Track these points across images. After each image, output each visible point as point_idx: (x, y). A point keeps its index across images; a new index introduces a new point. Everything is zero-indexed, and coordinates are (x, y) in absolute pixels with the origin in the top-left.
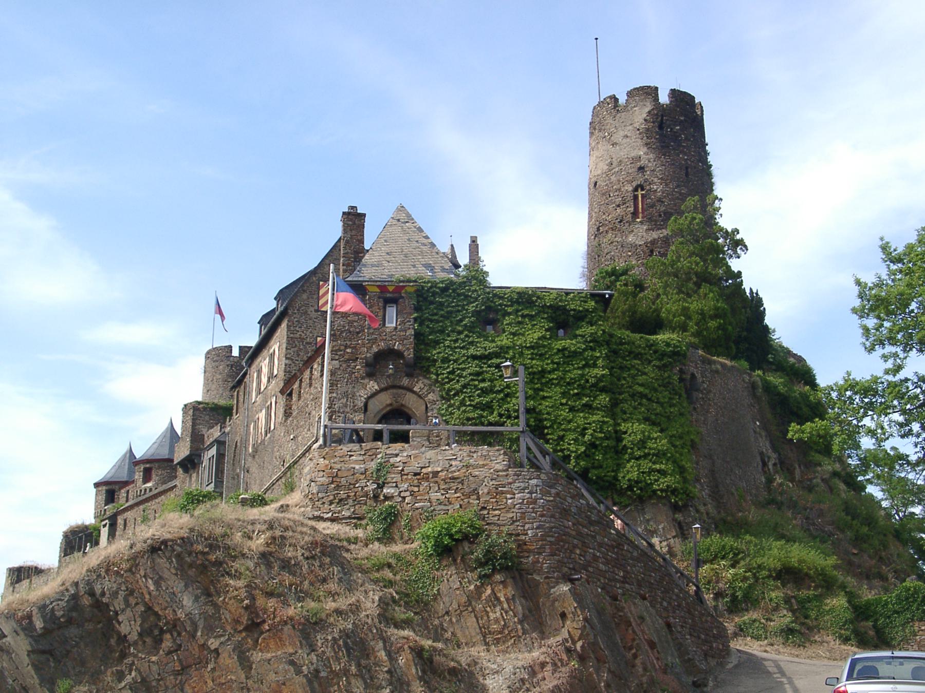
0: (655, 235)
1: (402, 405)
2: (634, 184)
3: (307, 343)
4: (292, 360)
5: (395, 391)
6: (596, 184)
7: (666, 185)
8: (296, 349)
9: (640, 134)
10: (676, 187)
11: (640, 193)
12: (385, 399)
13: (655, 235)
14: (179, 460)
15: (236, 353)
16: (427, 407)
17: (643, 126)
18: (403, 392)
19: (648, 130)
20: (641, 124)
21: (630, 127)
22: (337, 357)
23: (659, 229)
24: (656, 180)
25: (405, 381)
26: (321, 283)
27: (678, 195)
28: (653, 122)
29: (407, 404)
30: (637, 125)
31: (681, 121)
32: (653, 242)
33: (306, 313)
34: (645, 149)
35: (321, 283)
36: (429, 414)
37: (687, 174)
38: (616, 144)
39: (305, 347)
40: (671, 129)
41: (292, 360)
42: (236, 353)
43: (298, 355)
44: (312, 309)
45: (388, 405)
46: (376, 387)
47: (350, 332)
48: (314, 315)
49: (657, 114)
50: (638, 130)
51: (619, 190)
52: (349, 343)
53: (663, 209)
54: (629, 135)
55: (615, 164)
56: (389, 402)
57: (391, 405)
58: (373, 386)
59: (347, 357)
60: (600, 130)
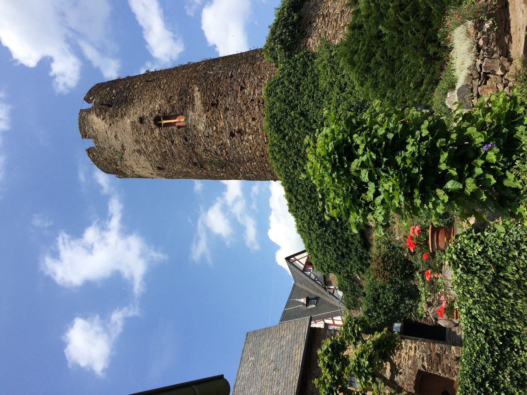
0: (198, 103)
2: (153, 126)
6: (159, 168)
10: (160, 87)
13: (198, 103)
19: (111, 116)
20: (106, 122)
21: (109, 133)
23: (193, 100)
24: (151, 106)
27: (166, 86)
30: (107, 126)
32: (204, 104)
34: (126, 117)
38: (123, 146)
40: (114, 96)
49: (100, 109)
50: (110, 125)
51: (159, 142)
53: (176, 97)
54: (114, 134)
55: (138, 147)
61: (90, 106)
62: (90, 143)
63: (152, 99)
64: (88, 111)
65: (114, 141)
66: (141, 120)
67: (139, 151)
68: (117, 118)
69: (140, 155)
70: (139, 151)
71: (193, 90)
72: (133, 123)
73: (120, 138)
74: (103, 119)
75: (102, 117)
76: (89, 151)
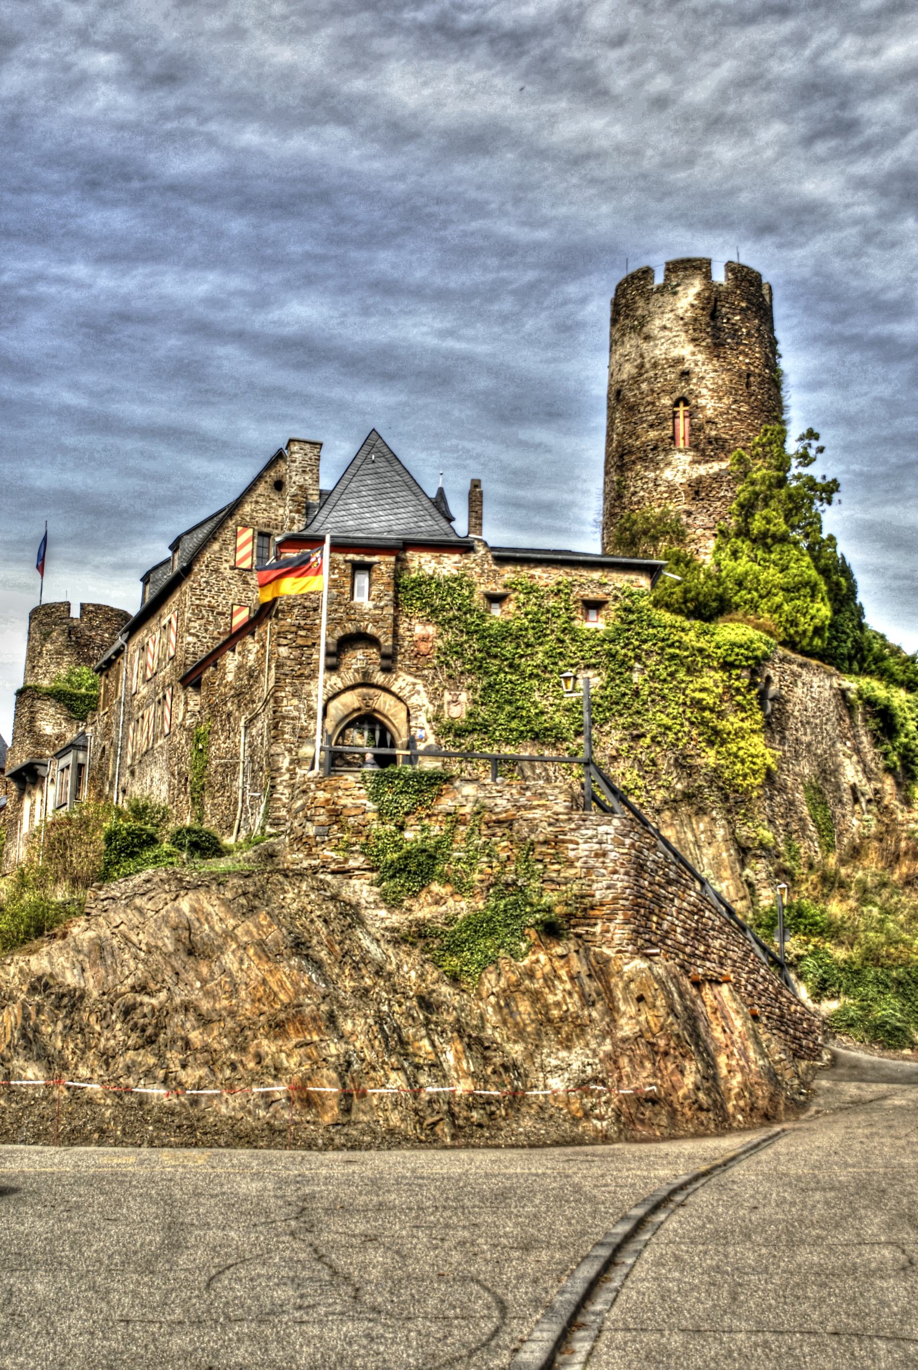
0: (703, 470)
1: (375, 710)
2: (677, 395)
3: (219, 613)
4: (198, 636)
5: (364, 690)
6: (619, 392)
7: (720, 399)
8: (203, 621)
9: (685, 324)
11: (681, 409)
12: (351, 700)
13: (703, 470)
14: (14, 770)
15: (75, 613)
16: (409, 714)
17: (689, 314)
18: (378, 692)
19: (695, 320)
20: (686, 311)
21: (671, 315)
22: (285, 642)
23: (707, 462)
24: (704, 391)
25: (379, 678)
26: (240, 529)
28: (703, 309)
29: (381, 709)
30: (680, 312)
31: (742, 309)
32: (699, 480)
33: (217, 571)
34: (690, 348)
35: (240, 529)
36: (412, 724)
37: (748, 385)
39: (216, 620)
40: (729, 319)
41: (198, 636)
42: (75, 613)
43: (206, 630)
44: (226, 565)
45: (355, 710)
46: (340, 685)
47: (305, 607)
48: (228, 573)
50: (682, 319)
51: (653, 404)
52: (302, 623)
53: (713, 433)
54: (668, 326)
55: (648, 366)
56: (356, 705)
57: (359, 709)
58: (336, 682)
59: (300, 641)
60: (627, 316)
61: (719, 276)
62: (659, 280)
63: (716, 391)
64: (708, 276)
65: (658, 323)
66: (685, 375)
67: (641, 366)
68: (691, 332)
69: (637, 367)
70: (641, 366)
71: (722, 460)
72: (680, 361)
73: (662, 334)
74: (692, 306)
75: (696, 302)
76: (646, 273)
